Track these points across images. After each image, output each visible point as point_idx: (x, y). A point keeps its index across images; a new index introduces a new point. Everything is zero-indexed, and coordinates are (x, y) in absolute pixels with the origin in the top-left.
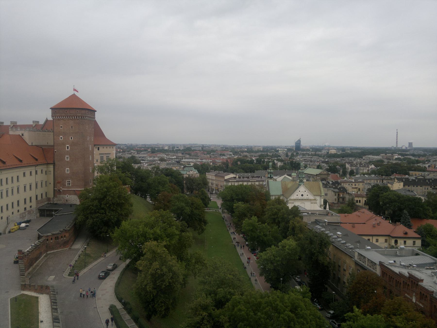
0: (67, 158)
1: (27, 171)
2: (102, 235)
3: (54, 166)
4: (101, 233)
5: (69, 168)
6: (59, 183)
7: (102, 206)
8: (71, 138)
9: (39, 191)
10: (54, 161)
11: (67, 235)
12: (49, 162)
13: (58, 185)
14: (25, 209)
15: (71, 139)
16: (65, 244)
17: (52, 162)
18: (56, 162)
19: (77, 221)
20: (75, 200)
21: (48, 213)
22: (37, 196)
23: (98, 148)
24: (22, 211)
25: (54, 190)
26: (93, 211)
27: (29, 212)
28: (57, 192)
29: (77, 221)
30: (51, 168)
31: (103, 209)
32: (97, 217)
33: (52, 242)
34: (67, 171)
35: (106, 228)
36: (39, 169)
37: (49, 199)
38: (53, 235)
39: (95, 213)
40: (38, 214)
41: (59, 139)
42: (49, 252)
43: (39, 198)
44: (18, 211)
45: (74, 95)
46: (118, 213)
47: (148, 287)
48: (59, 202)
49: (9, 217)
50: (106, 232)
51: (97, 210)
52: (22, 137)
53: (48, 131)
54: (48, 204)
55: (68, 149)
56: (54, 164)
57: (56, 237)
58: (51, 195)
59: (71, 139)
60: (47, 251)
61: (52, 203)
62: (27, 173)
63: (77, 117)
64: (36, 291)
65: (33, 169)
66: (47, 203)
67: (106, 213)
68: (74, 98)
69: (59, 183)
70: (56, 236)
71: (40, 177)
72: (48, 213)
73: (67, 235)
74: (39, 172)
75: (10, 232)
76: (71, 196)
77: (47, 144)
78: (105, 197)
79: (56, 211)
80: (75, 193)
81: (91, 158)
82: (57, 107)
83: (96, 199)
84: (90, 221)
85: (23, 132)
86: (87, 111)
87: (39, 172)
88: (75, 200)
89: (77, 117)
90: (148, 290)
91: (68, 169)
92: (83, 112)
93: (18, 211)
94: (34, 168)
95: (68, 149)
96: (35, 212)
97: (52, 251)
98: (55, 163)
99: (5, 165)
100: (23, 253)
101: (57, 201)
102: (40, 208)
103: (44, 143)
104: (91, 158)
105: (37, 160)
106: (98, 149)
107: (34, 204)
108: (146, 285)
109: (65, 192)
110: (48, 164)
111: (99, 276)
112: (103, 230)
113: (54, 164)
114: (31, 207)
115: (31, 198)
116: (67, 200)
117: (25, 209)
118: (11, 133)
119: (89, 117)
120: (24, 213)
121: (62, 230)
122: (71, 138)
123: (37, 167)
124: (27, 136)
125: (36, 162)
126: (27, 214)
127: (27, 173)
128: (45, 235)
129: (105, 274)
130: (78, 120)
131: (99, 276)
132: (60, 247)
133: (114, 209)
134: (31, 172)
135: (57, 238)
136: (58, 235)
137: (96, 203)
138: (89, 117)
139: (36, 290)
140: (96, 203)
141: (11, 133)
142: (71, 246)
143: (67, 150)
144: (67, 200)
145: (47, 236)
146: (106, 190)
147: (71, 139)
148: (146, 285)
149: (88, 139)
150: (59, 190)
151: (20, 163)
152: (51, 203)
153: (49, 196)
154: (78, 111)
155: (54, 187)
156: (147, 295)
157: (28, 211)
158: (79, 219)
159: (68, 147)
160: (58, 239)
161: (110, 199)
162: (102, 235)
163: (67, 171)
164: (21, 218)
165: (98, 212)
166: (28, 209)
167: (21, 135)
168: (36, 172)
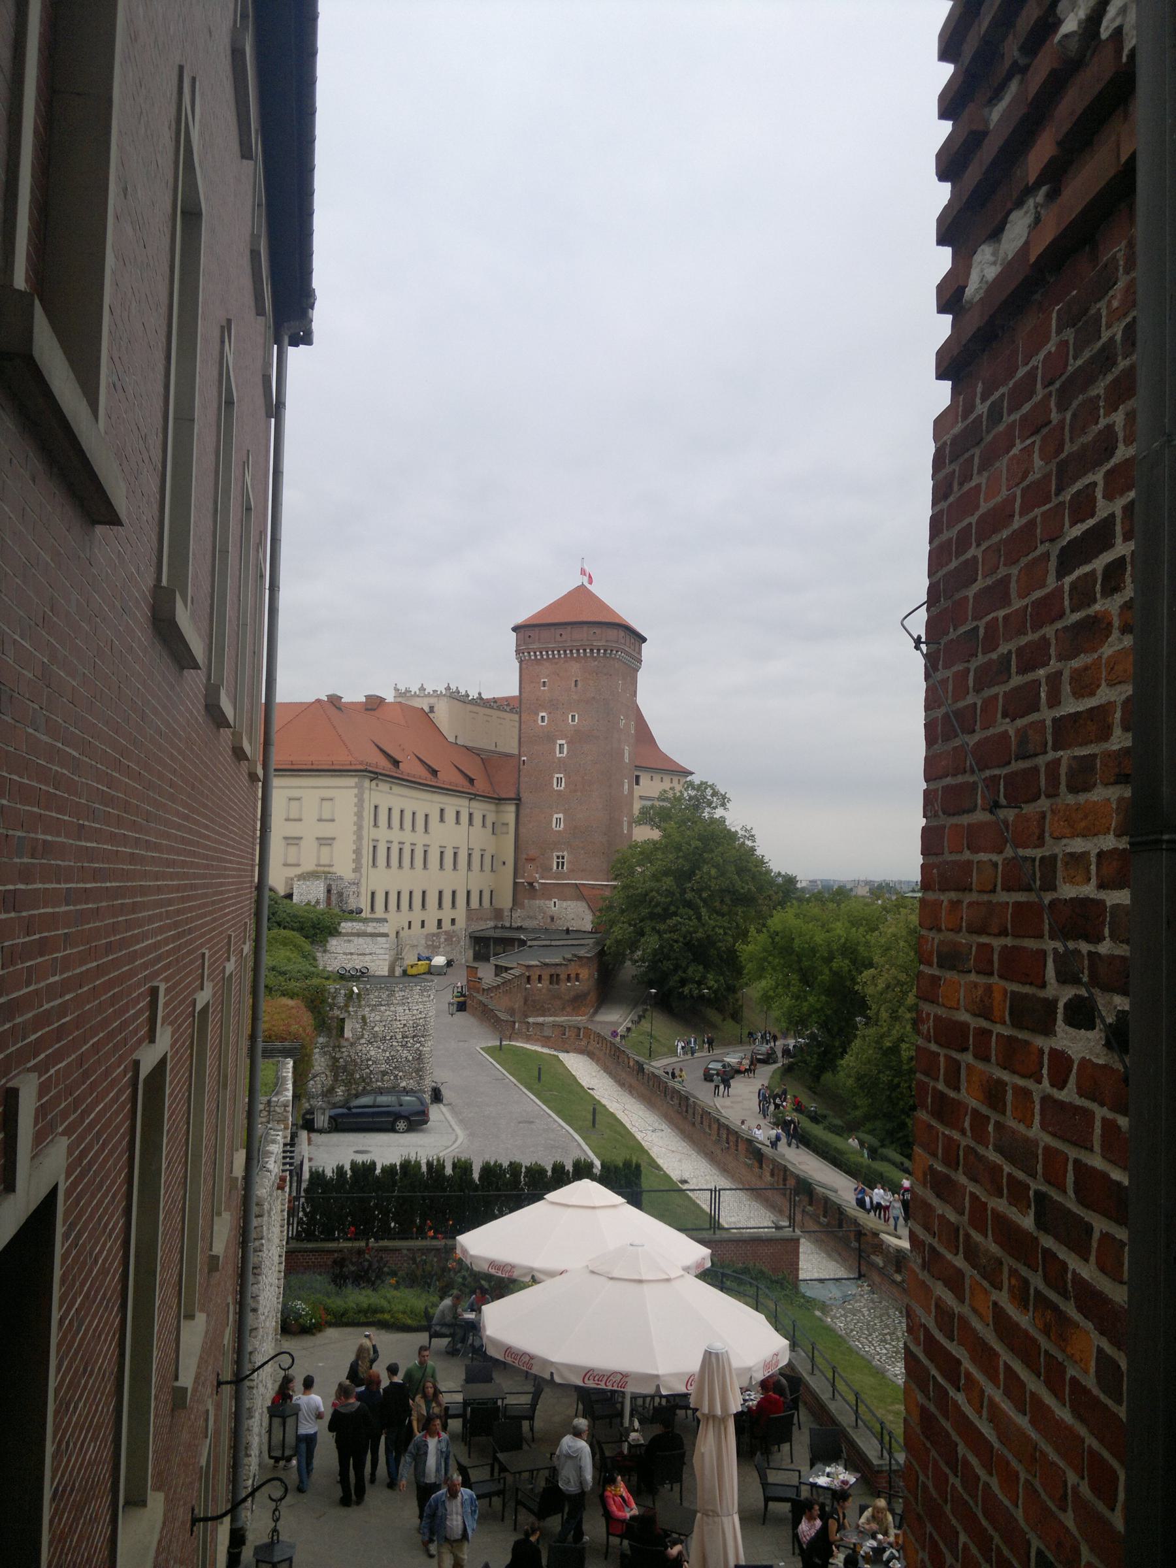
0: (559, 783)
1: (453, 804)
2: (686, 990)
3: (518, 806)
4: (683, 982)
6: (531, 860)
7: (689, 896)
8: (573, 717)
9: (479, 881)
11: (584, 973)
12: (504, 796)
13: (530, 867)
14: (440, 921)
15: (573, 720)
16: (576, 1002)
17: (513, 796)
18: (525, 796)
19: (608, 942)
20: (577, 915)
22: (468, 892)
23: (637, 777)
24: (431, 927)
25: (515, 883)
26: (659, 910)
27: (450, 936)
28: (524, 891)
29: (608, 942)
31: (689, 904)
32: (673, 930)
33: (540, 990)
34: (558, 821)
35: (701, 968)
36: (479, 808)
37: (498, 914)
38: (546, 965)
39: (666, 915)
40: (471, 953)
41: (536, 721)
43: (475, 903)
45: (582, 587)
46: (738, 926)
47: (904, 1046)
48: (526, 924)
49: (402, 934)
50: (699, 983)
51: (673, 908)
52: (431, 715)
53: (498, 709)
54: (496, 927)
56: (518, 801)
57: (551, 976)
58: (505, 901)
59: (573, 720)
61: (508, 925)
62: (450, 816)
63: (592, 650)
64: (546, 1041)
65: (463, 804)
66: (491, 924)
67: (699, 918)
68: (581, 594)
69: (531, 860)
70: (553, 972)
71: (479, 838)
73: (584, 973)
74: (478, 820)
75: (405, 973)
76: (565, 904)
77: (493, 748)
78: (690, 875)
80: (579, 893)
81: (626, 787)
82: (532, 622)
83: (666, 873)
84: (652, 942)
86: (622, 634)
87: (478, 820)
88: (577, 915)
89: (592, 650)
90: (905, 1055)
91: (561, 816)
92: (612, 634)
94: (465, 802)
96: (462, 943)
98: (519, 799)
101: (523, 920)
102: (477, 934)
103: (483, 742)
104: (626, 787)
105: (471, 781)
106: (637, 783)
107: (460, 913)
108: (895, 1050)
109: (548, 892)
110: (499, 801)
111: (707, 1070)
112: (690, 970)
113: (518, 801)
114: (453, 921)
115: (454, 893)
116: (552, 919)
117: (440, 921)
119: (627, 653)
120: (437, 935)
121: (569, 956)
122: (573, 717)
123: (474, 804)
124: (443, 716)
125: (468, 789)
126: (442, 940)
127: (450, 816)
129: (724, 1066)
130: (595, 659)
131: (707, 1070)
132: (563, 1009)
133: (725, 909)
134: (458, 813)
135: (554, 979)
136: (559, 970)
137: (668, 882)
138: (627, 653)
139: (548, 1038)
140: (668, 882)
142: (596, 1012)
144: (552, 919)
145: (528, 967)
146: (699, 844)
147: (573, 720)
148: (895, 1050)
149: (622, 723)
150: (531, 884)
151: (429, 781)
152: (503, 927)
153: (498, 904)
154: (598, 631)
156: (898, 1086)
158: (617, 932)
160: (557, 983)
161: (713, 872)
162: (686, 990)
163: (558, 821)
164: (428, 947)
165: (675, 914)
166: (447, 925)
167: (427, 709)
168: (471, 815)
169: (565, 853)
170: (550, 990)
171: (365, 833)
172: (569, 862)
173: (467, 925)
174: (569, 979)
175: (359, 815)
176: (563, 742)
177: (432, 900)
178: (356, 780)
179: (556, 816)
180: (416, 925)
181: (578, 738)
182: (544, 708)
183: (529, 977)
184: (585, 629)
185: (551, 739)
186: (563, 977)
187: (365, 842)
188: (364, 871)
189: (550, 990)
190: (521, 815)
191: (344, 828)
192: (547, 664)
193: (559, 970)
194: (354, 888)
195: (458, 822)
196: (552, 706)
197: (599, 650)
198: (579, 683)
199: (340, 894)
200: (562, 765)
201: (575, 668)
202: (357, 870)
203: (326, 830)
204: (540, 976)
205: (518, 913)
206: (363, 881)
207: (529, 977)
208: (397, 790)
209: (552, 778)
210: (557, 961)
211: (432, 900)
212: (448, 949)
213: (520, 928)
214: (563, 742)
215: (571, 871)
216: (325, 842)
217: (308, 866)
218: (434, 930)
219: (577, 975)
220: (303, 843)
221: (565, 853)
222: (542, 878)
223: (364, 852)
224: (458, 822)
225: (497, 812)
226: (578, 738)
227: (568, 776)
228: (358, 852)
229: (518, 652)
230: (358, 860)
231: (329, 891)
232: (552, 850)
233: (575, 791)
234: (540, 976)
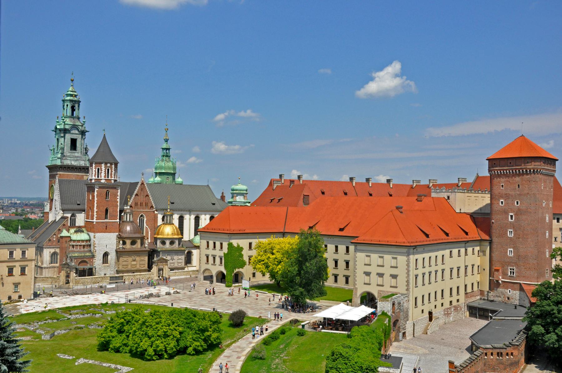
5: (513, 248)
8: (517, 203)
12: (483, 238)
14: (451, 302)
15: (517, 204)
21: (482, 313)
22: (466, 286)
24: (447, 305)
25: (490, 279)
27: (456, 308)
28: (494, 285)
33: (492, 360)
37: (482, 293)
38: (495, 348)
41: (498, 204)
44: (442, 304)
48: (496, 299)
55: (512, 219)
57: (498, 353)
61: (486, 298)
70: (498, 351)
72: (482, 313)
79: (493, 312)
81: (547, 234)
85: (449, 194)
91: (512, 249)
93: (442, 304)
95: (512, 219)
99: (428, 239)
100: (455, 368)
104: (547, 234)
114: (458, 301)
116: (508, 298)
117: (451, 302)
118: (433, 195)
120: (450, 308)
126: (452, 310)
128: (482, 346)
136: (502, 351)
141: (433, 195)
144: (508, 298)
147: (517, 204)
149: (544, 205)
152: (484, 299)
155: (490, 277)
157: (454, 307)
159: (512, 216)
164: (445, 314)
166: (455, 303)
169: (514, 268)
171: (411, 273)
172: (517, 272)
173: (465, 300)
174: (507, 354)
175: (408, 265)
177: (447, 293)
178: (407, 250)
179: (509, 249)
180: (439, 305)
181: (519, 212)
182: (502, 198)
185: (506, 213)
187: (411, 277)
188: (411, 290)
191: (401, 272)
193: (502, 351)
194: (406, 299)
195: (459, 256)
196: (507, 197)
199: (399, 303)
200: (512, 226)
202: (407, 290)
203: (394, 272)
205: (492, 293)
206: (411, 294)
207: (486, 354)
208: (427, 248)
209: (507, 231)
210: (501, 345)
211: (447, 293)
212: (456, 313)
213: (493, 301)
215: (518, 276)
216: (394, 277)
217: (387, 289)
218: (449, 306)
220: (384, 276)
221: (514, 268)
222: (503, 278)
223: (411, 281)
224: (459, 256)
226: (519, 212)
228: (408, 282)
230: (408, 285)
231: (393, 304)
232: (508, 266)
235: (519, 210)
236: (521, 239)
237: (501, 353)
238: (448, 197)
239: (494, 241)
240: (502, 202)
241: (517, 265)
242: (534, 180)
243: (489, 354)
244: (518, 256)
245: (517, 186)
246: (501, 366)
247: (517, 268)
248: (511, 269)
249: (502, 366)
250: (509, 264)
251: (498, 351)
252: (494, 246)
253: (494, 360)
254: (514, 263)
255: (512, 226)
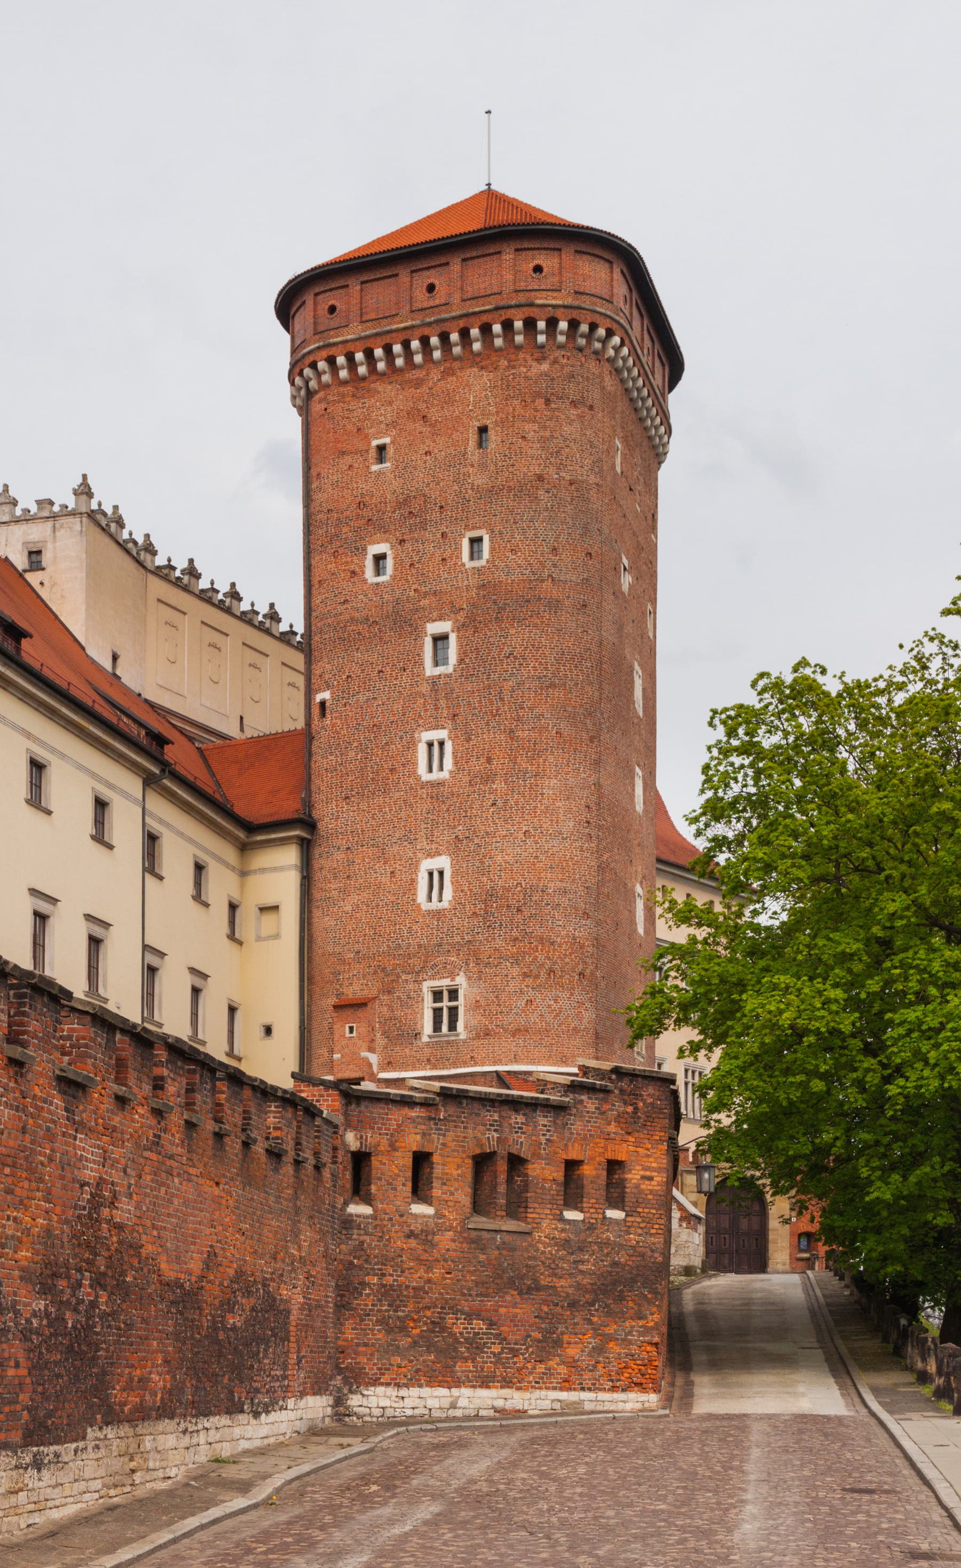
3: (306, 846)
5: (456, 848)
6: (351, 1007)
10: (308, 804)
13: (348, 1032)
17: (288, 807)
30: (286, 858)
33: (424, 1235)
34: (434, 881)
42: (375, 1400)
52: (33, 578)
57: (482, 1162)
59: (472, 558)
60: (357, 1379)
63: (530, 324)
69: (351, 1007)
70: (484, 1133)
86: (621, 289)
89: (530, 324)
91: (443, 862)
97: (430, 1399)
98: (310, 825)
113: (305, 829)
130: (541, 353)
132: (549, 1344)
135: (497, 1177)
143: (430, 670)
169: (461, 980)
170: (476, 1241)
176: (443, 627)
179: (427, 864)
183: (360, 1160)
184: (508, 256)
185: (402, 620)
186: (544, 1172)
189: (476, 1241)
190: (318, 876)
192: (386, 389)
193: (522, 1133)
197: (552, 323)
198: (493, 436)
201: (476, 388)
204: (421, 1160)
207: (360, 1160)
209: (412, 745)
214: (443, 627)
219: (614, 1166)
221: (461, 980)
222: (389, 1064)
225: (244, 874)
226: (487, 610)
227: (464, 735)
229: (295, 370)
232: (418, 975)
233: (488, 778)
234: (421, 1160)
235: (487, 587)
236: (499, 785)
237: (516, 1162)
238: (35, 556)
239: (326, 825)
240: (379, 559)
241: (475, 958)
242: (572, 391)
243: (392, 1169)
244: (489, 903)
245: (473, 438)
246: (518, 1310)
247: (476, 978)
248: (437, 996)
249: (525, 1310)
250: (426, 960)
251: (484, 1133)
252: (329, 860)
253: (445, 1240)
254: (457, 948)
255: (442, 701)
